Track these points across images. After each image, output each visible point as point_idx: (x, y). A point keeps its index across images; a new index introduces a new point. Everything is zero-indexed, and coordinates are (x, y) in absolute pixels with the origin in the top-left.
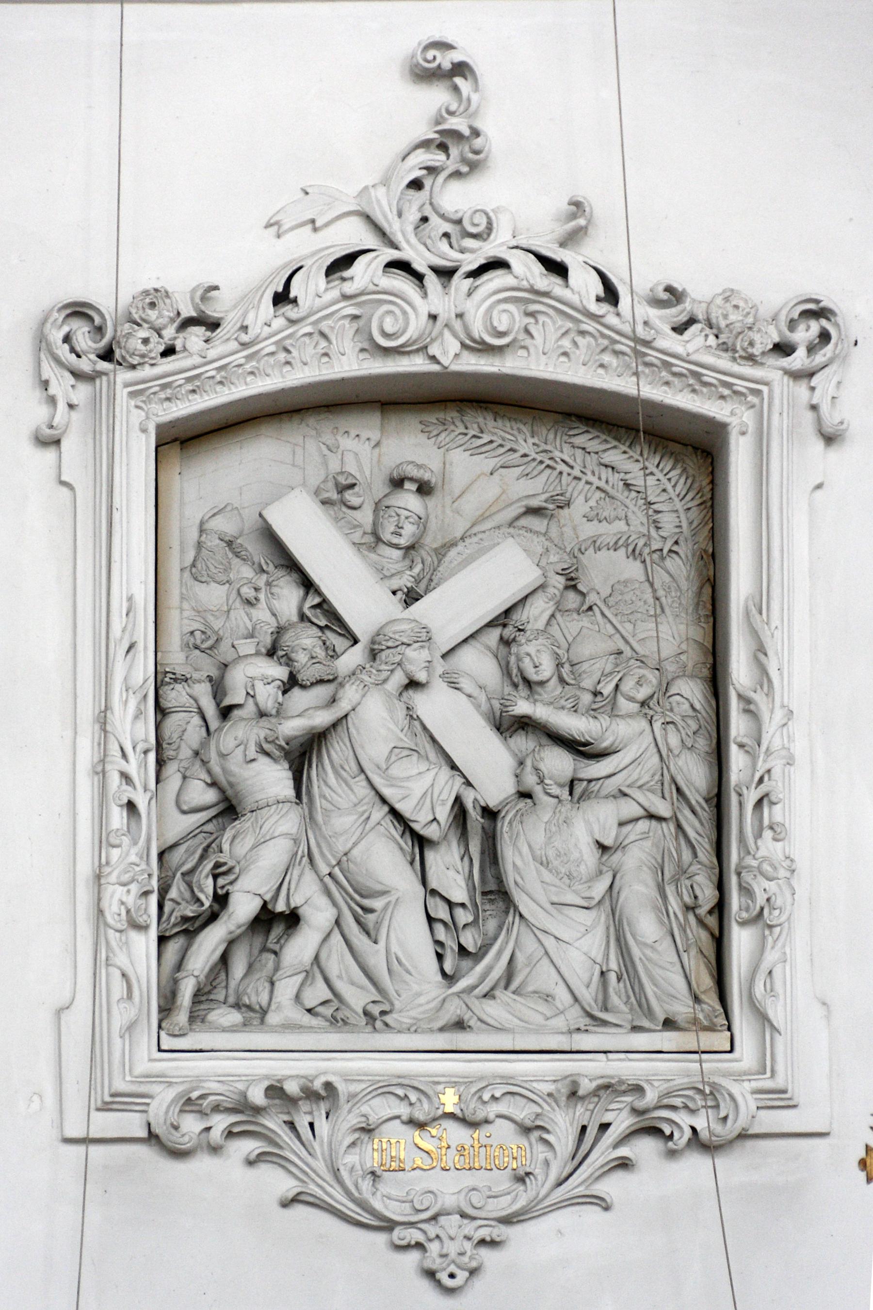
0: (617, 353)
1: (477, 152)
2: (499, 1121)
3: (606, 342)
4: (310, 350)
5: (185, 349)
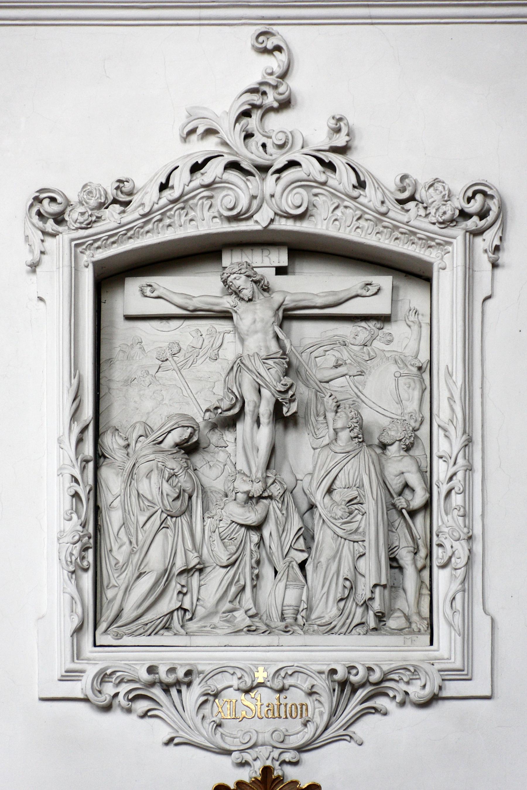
0: (367, 220)
2: (291, 688)
4: (183, 218)
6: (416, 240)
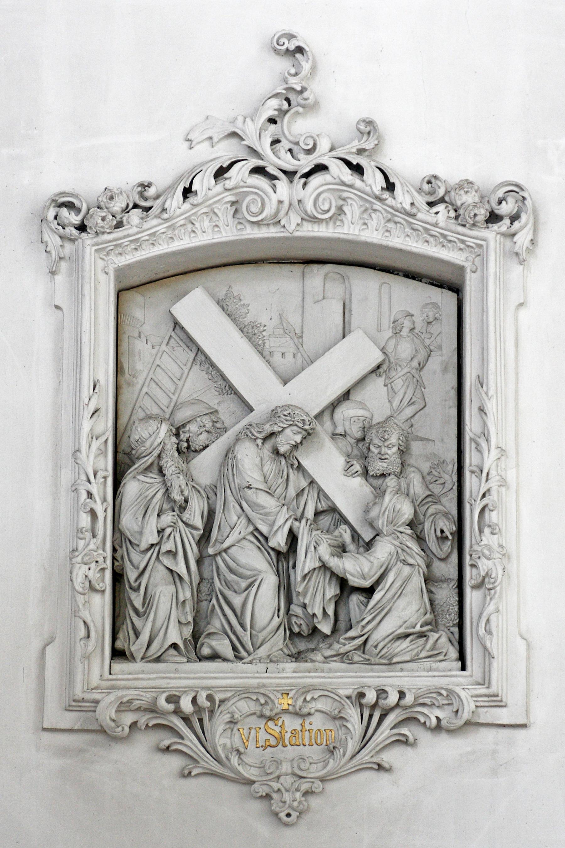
1: (305, 99)
2: (317, 714)
6: (445, 243)
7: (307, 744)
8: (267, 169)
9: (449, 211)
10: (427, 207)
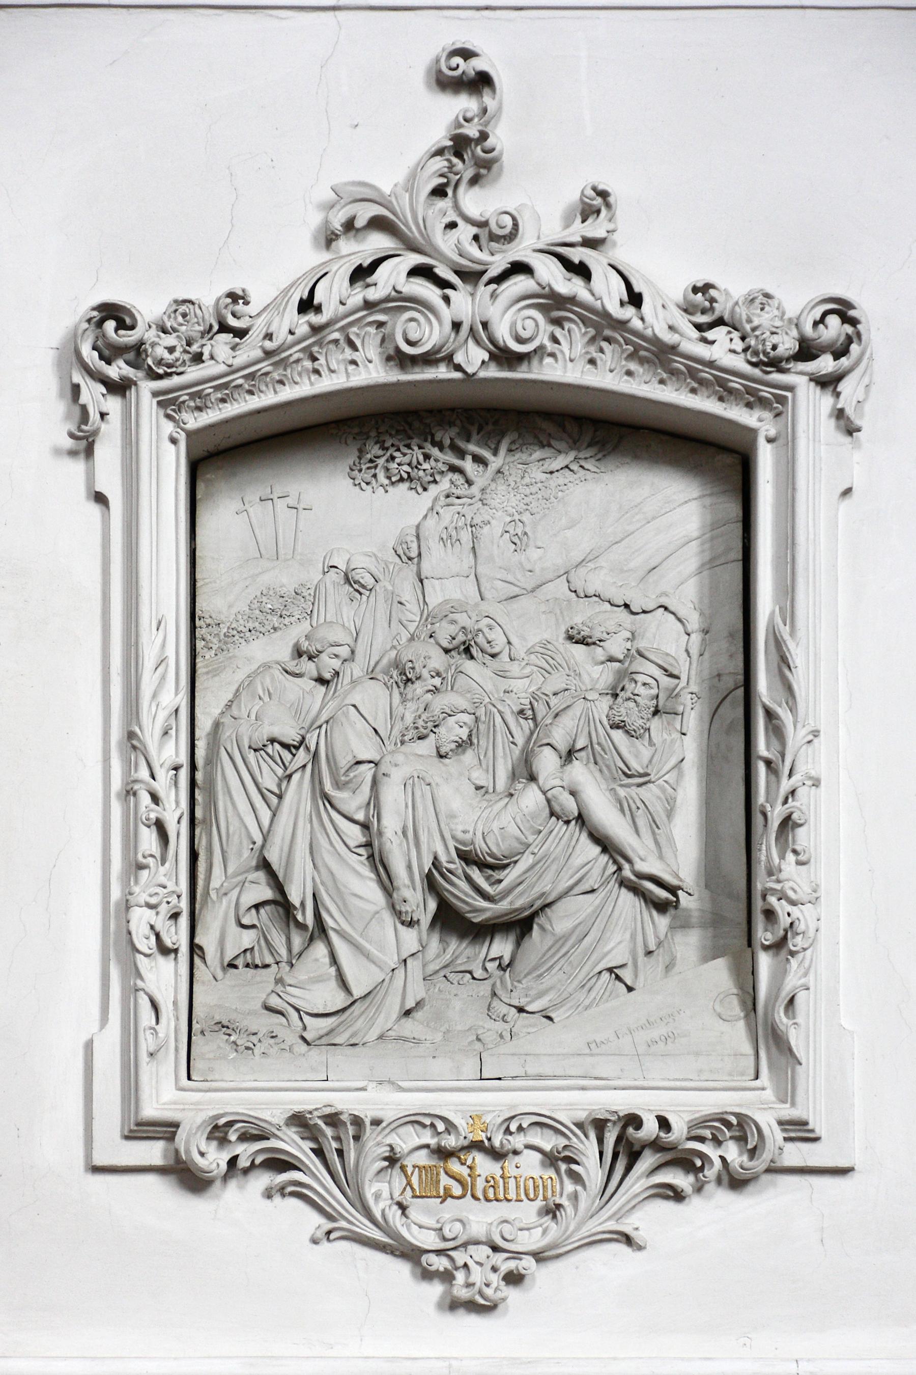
2: (526, 1151)
3: (631, 348)
5: (212, 358)
7: (515, 1198)
8: (437, 271)
9: (731, 340)
10: (695, 334)
